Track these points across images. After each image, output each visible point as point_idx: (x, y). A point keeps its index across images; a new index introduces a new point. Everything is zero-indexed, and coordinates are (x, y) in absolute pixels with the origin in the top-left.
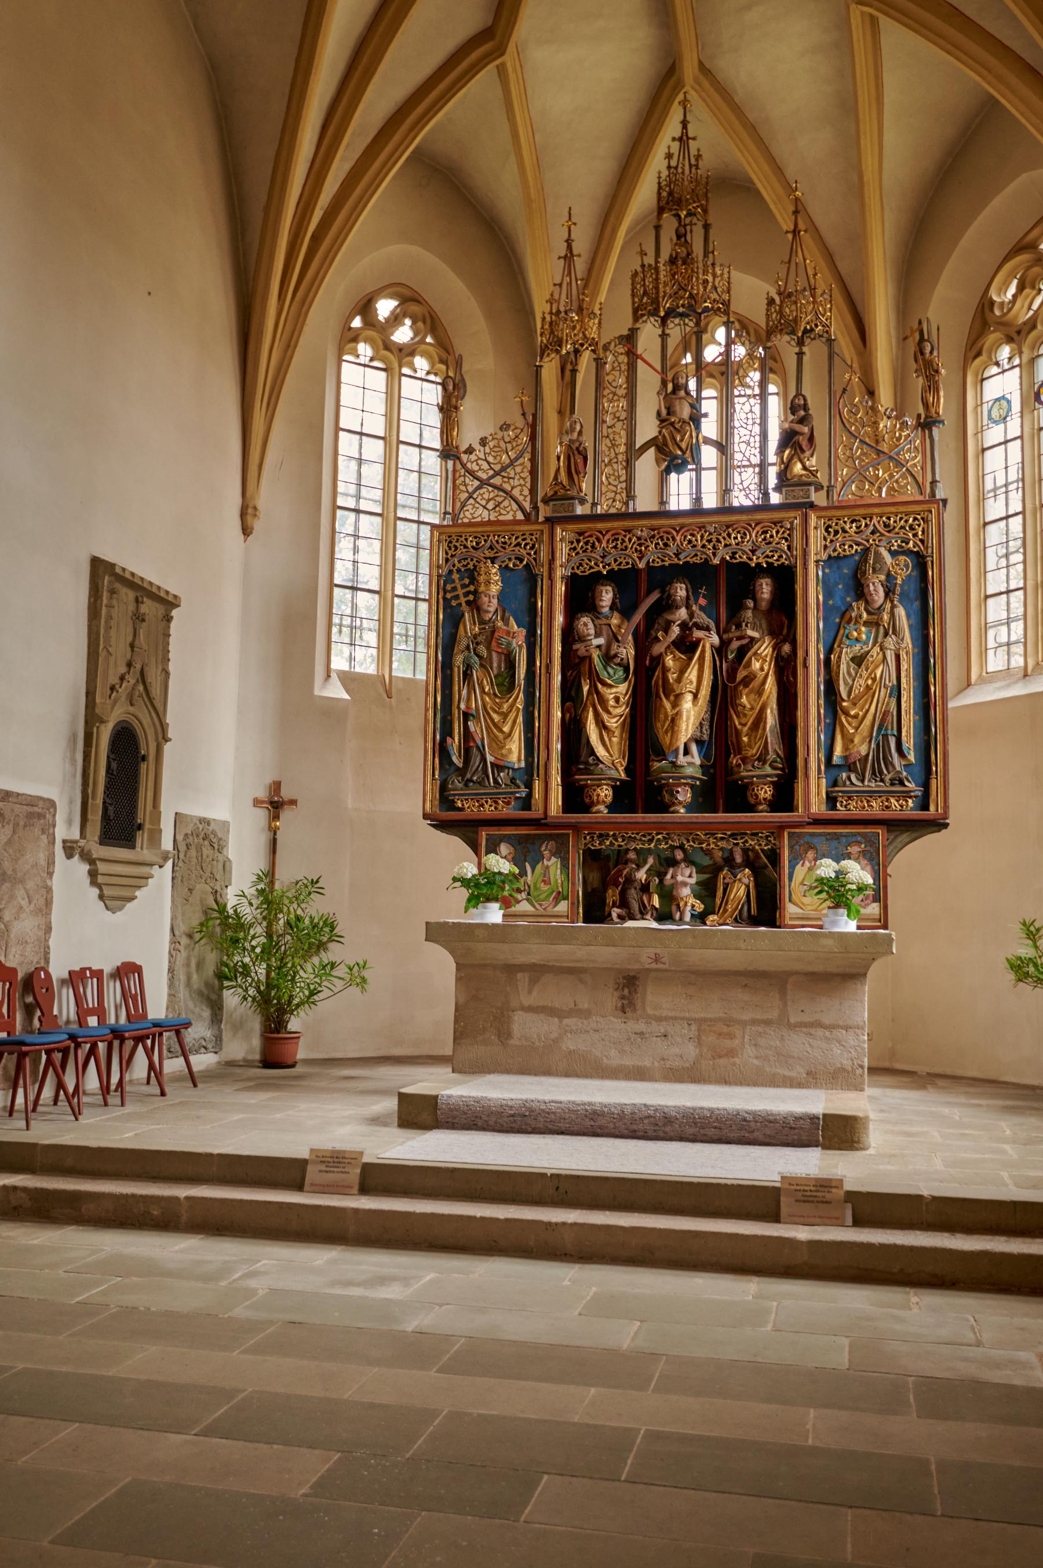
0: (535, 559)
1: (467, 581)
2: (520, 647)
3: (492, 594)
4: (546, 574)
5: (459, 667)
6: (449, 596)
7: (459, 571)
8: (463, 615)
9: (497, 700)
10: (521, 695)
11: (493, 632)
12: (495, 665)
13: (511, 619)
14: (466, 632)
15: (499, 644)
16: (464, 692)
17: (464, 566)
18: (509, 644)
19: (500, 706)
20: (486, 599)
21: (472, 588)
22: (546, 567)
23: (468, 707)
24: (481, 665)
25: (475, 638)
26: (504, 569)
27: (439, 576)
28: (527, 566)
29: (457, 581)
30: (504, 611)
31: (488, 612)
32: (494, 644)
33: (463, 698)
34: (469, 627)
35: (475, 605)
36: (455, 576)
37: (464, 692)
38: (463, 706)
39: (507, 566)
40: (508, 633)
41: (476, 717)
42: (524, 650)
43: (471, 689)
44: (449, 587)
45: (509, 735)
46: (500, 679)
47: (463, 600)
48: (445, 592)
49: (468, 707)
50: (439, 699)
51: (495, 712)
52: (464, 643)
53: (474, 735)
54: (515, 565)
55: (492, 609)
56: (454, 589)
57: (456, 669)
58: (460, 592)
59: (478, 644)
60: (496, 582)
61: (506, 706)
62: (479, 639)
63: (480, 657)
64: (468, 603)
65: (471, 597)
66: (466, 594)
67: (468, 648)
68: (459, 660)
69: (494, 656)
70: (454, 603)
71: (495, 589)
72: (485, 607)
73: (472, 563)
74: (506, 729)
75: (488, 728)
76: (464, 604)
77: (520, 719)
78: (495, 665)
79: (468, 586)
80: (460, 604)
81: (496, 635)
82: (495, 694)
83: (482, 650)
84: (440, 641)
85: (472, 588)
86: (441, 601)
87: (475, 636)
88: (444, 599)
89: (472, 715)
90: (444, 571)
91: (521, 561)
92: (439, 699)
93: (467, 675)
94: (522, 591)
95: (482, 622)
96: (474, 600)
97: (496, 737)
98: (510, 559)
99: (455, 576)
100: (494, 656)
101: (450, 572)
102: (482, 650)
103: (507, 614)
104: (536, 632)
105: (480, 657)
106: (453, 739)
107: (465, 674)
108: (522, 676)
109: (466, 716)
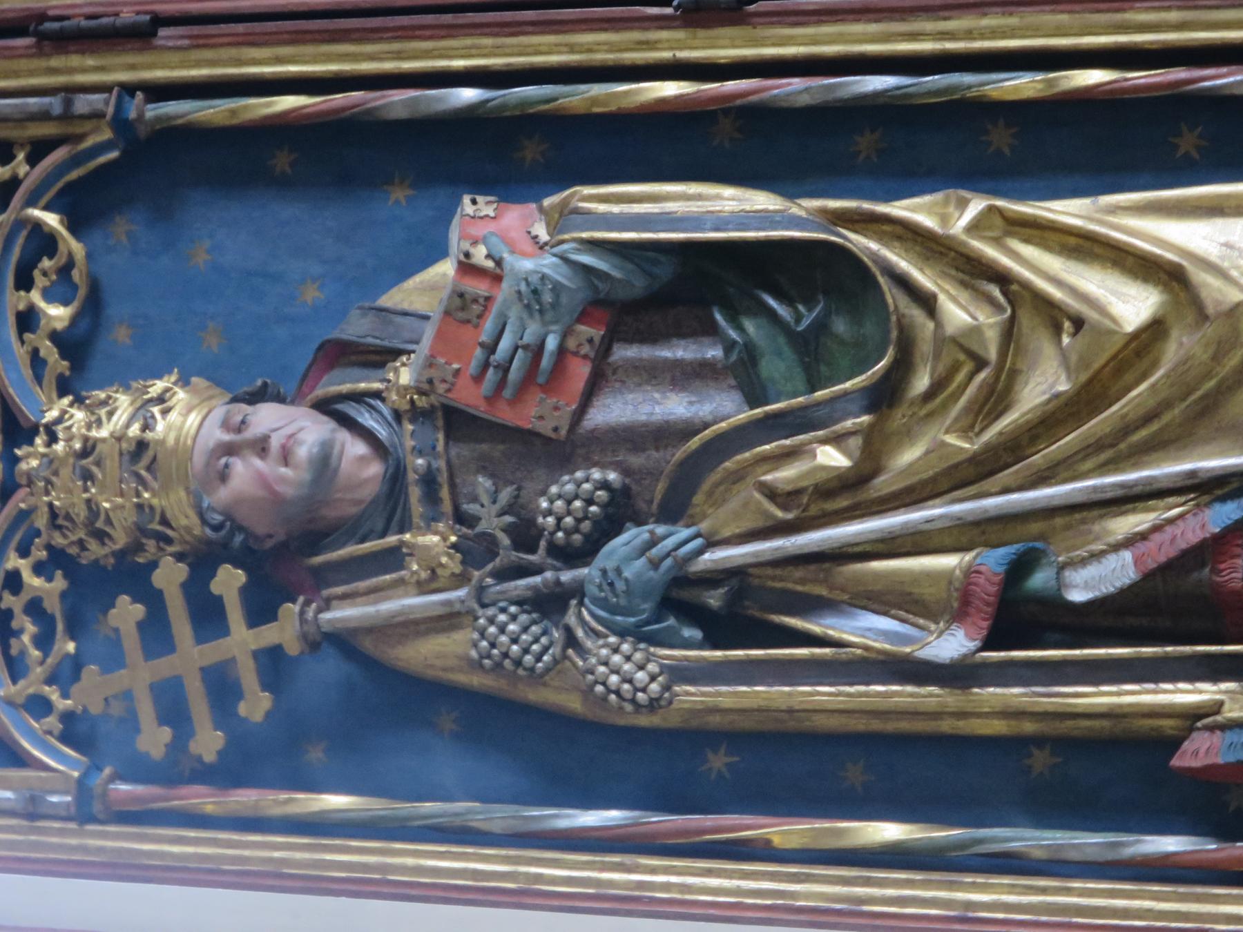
0: (38, 150)
1: (127, 613)
2: (562, 219)
3: (216, 435)
4: (122, 68)
5: (680, 674)
6: (208, 742)
7: (66, 675)
8: (342, 642)
9: (922, 382)
10: (916, 210)
11: (456, 422)
12: (675, 406)
13: (394, 298)
14: (448, 620)
15: (539, 374)
16: (865, 630)
17: (44, 641)
18: (535, 297)
19: (966, 349)
20: (243, 471)
21: (170, 576)
22: (86, 69)
23: (955, 604)
24: (674, 510)
25: (489, 546)
26: (80, 361)
27: (86, 810)
28: (82, 206)
29: (121, 679)
30: (339, 354)
31: (324, 463)
32: (542, 414)
33: (902, 639)
34: (416, 600)
35: (285, 553)
36: (91, 692)
37: (865, 630)
38: (951, 644)
39: (74, 345)
40: (462, 308)
41: (1029, 540)
42: (592, 198)
43: (825, 579)
44: (154, 739)
45: (1168, 274)
46: (777, 365)
47: (242, 640)
48: (178, 769)
49: (955, 604)
50: (889, 832)
51: (996, 399)
52: (513, 632)
53: (1161, 550)
54: (60, 291)
55: (308, 430)
56: (173, 710)
57: (691, 695)
58: (190, 655)
59: (525, 534)
60: (142, 411)
61: (958, 312)
62: (492, 522)
63: (618, 512)
64: (261, 610)
65: (229, 581)
66: (208, 616)
67: (548, 605)
68: (622, 669)
69: (616, 410)
70: (256, 705)
71: (185, 417)
72: (290, 479)
73: (33, 581)
74: (1132, 305)
75: (1116, 448)
76: (269, 635)
77: (1068, 211)
78: (675, 406)
79: (154, 601)
80: (273, 663)
81: (470, 397)
82: (883, 396)
83: (563, 498)
84: (500, 816)
85: (170, 576)
86: (245, 799)
87: (475, 551)
88: (227, 773)
89: (1021, 567)
90: (63, 763)
91: (45, 242)
92: (889, 832)
93: (738, 613)
94: (224, 236)
95: (391, 506)
96: (246, 558)
97: (1183, 384)
98: (27, 320)
99: (91, 692)
100: (616, 410)
101: (75, 732)
102: (563, 498)
103: (356, 328)
104: (468, 117)
105: (618, 512)
106: (1193, 717)
107: (720, 630)
108: (762, 200)
109: (1021, 617)
